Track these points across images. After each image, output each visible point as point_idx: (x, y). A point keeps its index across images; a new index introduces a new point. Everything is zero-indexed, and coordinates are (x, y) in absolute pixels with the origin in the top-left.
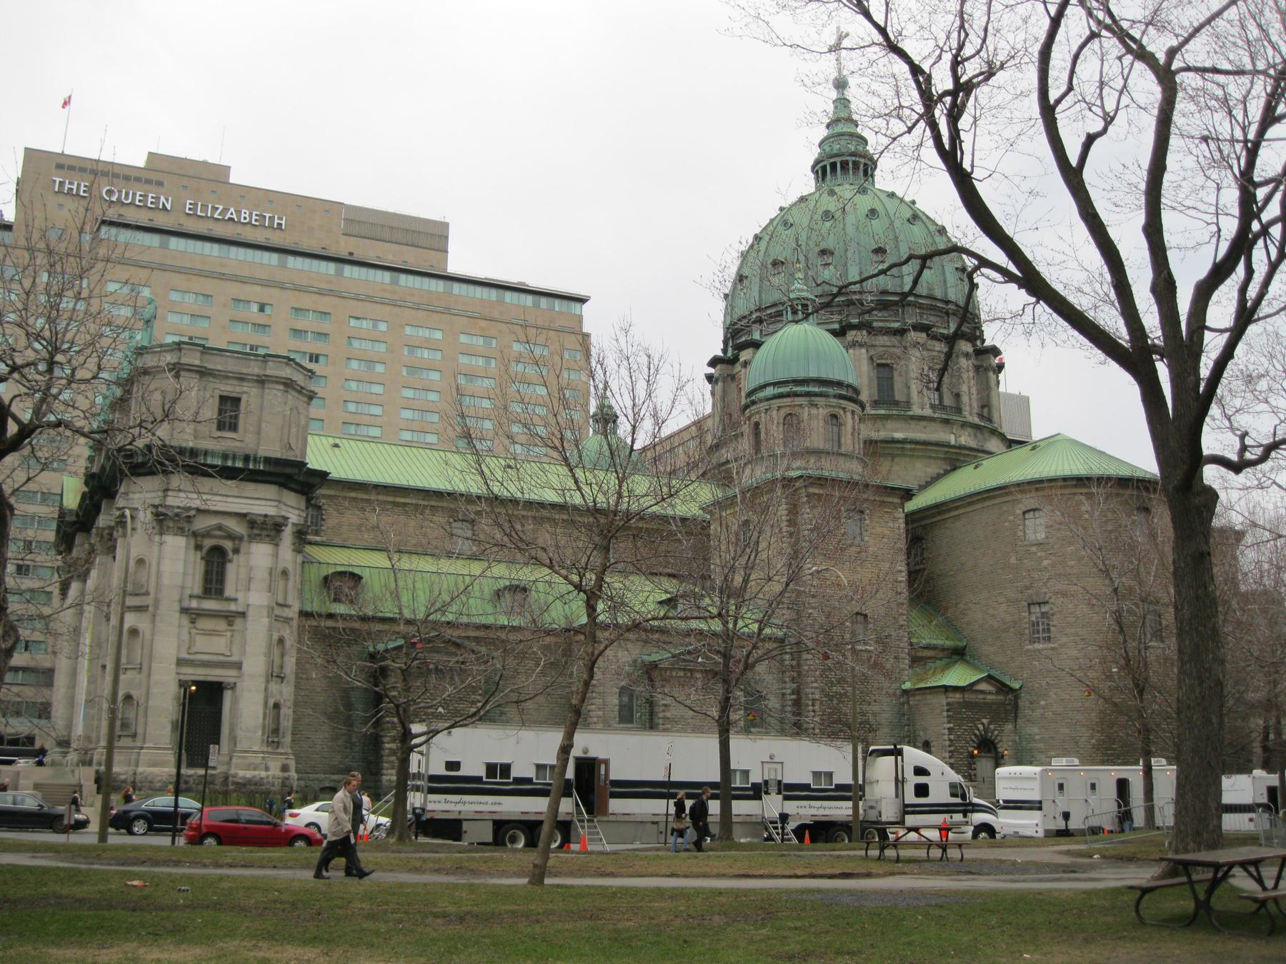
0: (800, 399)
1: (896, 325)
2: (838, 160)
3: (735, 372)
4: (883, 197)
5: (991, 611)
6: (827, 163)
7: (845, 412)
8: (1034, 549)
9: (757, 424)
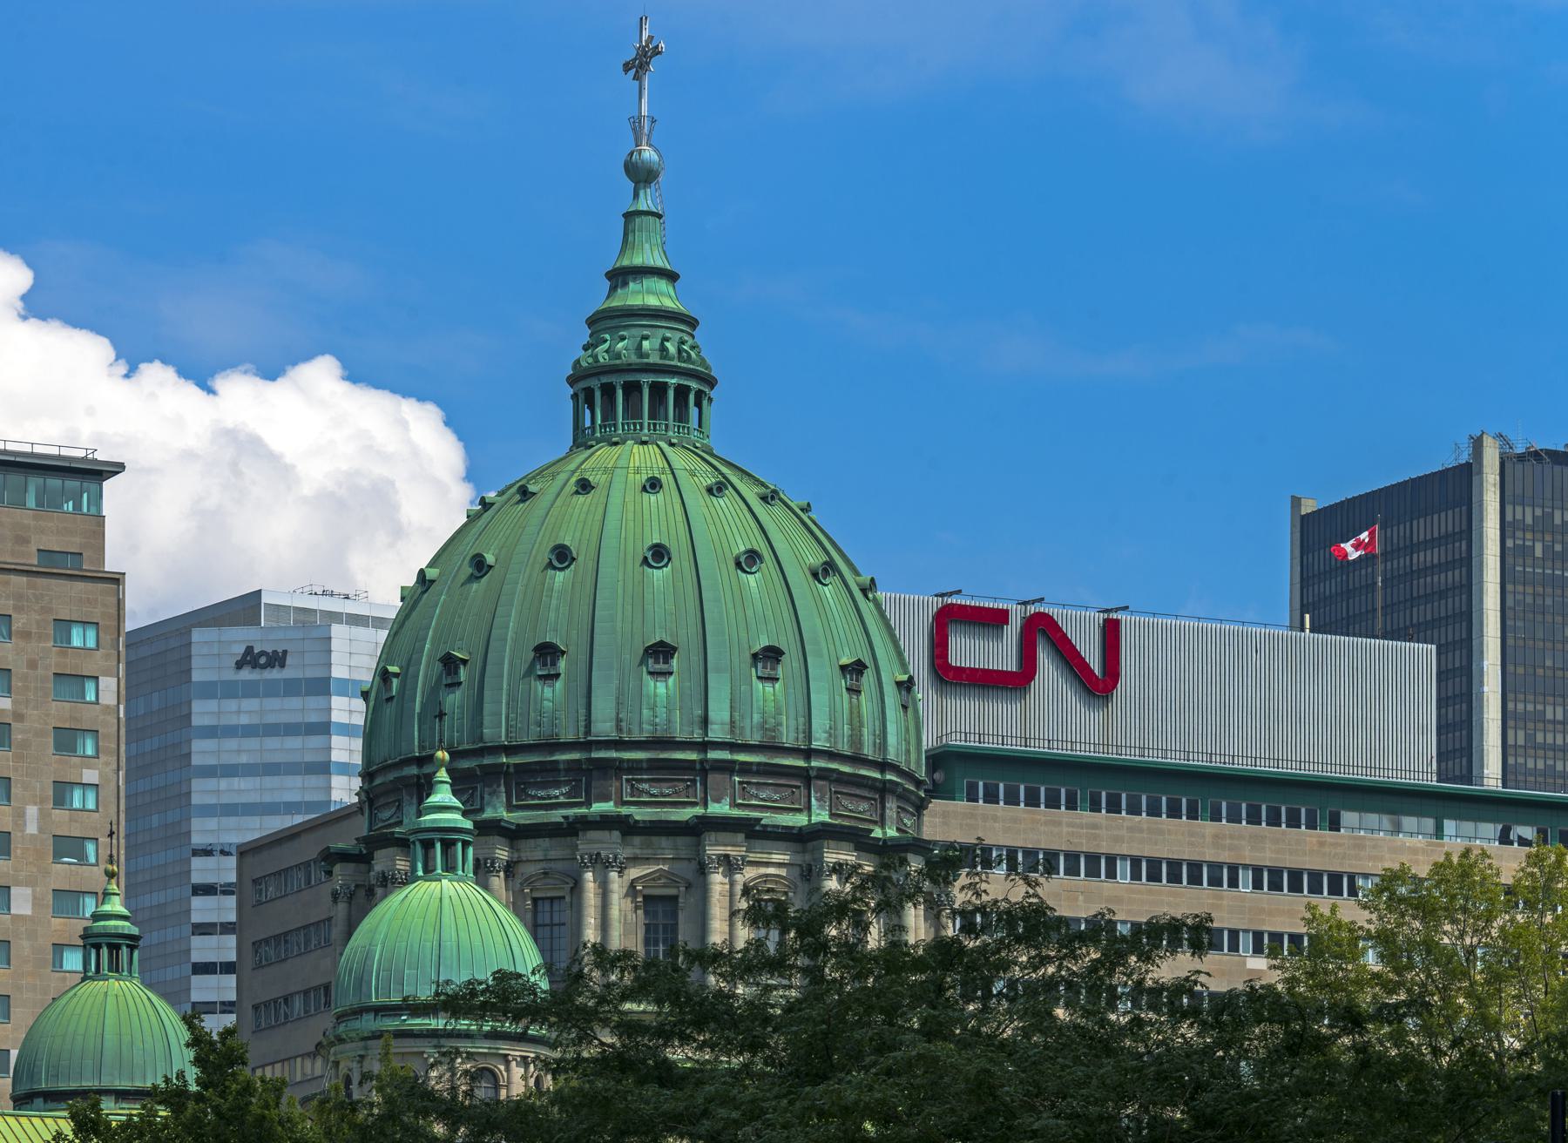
0: (419, 1042)
1: (686, 814)
2: (618, 380)
7: (507, 1063)
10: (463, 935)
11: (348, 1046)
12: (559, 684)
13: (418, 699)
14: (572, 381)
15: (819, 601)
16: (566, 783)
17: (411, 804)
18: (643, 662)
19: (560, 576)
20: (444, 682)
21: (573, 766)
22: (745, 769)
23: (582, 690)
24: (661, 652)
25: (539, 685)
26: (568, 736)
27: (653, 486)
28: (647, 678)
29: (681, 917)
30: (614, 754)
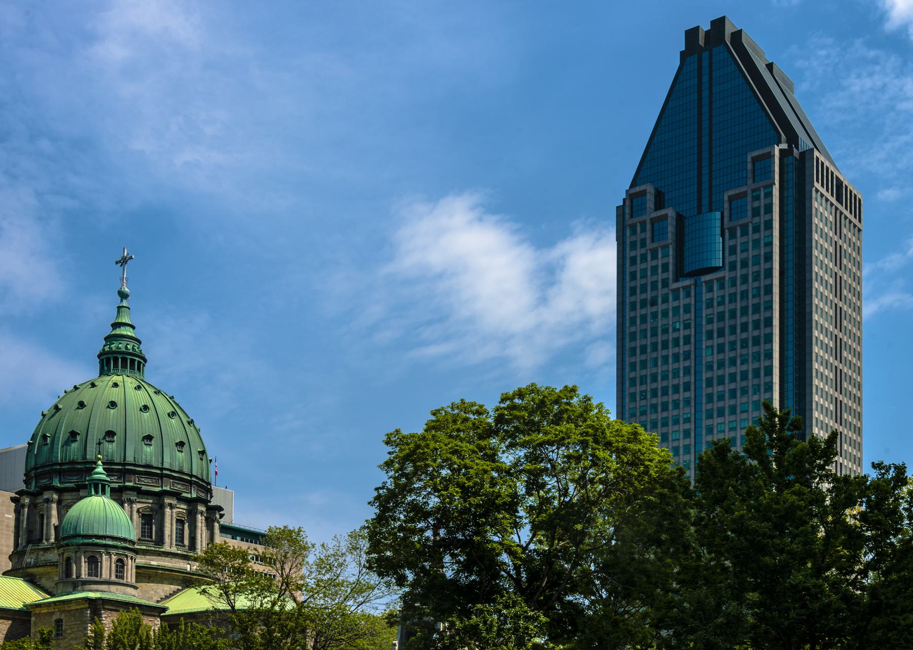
7: (127, 558)
10: (113, 514)
11: (71, 548)
12: (114, 444)
13: (60, 444)
14: (99, 356)
15: (191, 430)
16: (116, 475)
17: (56, 478)
18: (143, 440)
19: (112, 411)
20: (71, 439)
21: (118, 471)
22: (174, 478)
23: (123, 447)
24: (149, 438)
25: (107, 443)
26: (117, 460)
27: (139, 388)
28: (144, 445)
30: (132, 468)
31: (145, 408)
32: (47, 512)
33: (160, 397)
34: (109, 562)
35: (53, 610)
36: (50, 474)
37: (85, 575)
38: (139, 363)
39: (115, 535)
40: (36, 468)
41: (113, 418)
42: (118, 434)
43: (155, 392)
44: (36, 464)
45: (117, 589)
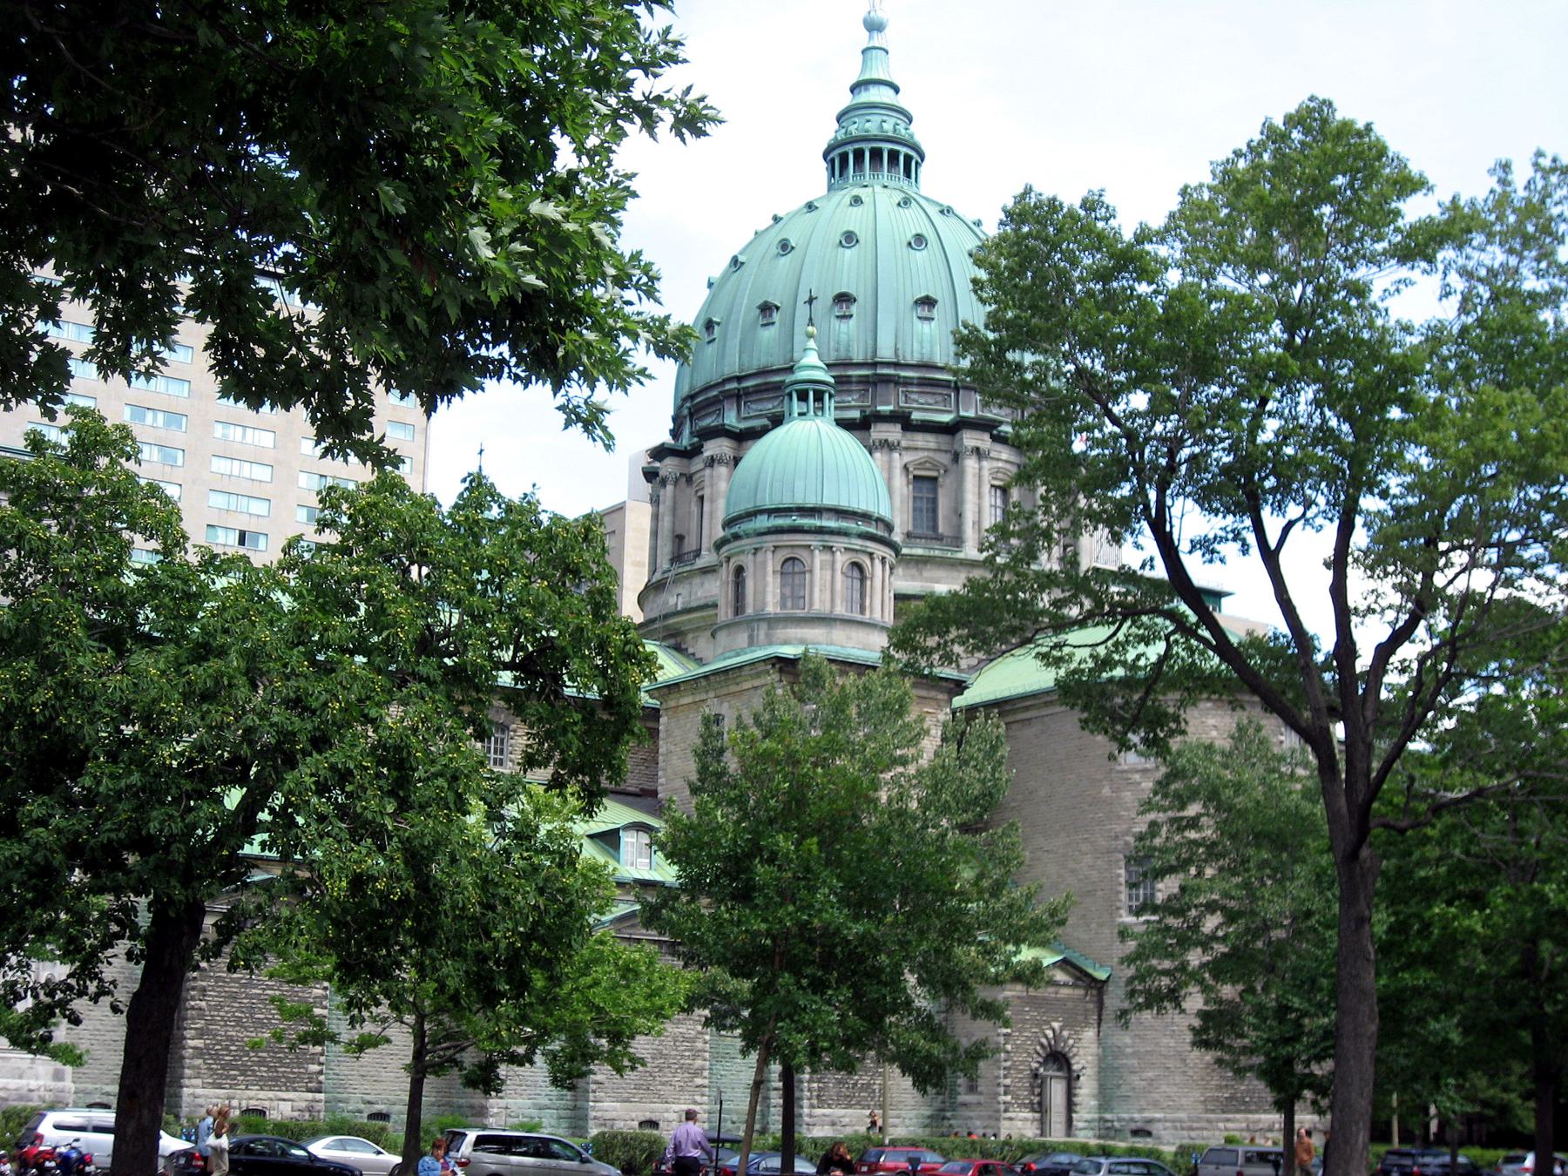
0: (807, 537)
1: (946, 418)
2: (867, 147)
3: (693, 470)
4: (933, 212)
5: (1071, 865)
6: (850, 149)
7: (872, 559)
8: (1137, 777)
9: (739, 570)
12: (852, 322)
19: (848, 252)
21: (864, 381)
24: (928, 302)
25: (837, 322)
26: (858, 357)
29: (941, 492)
31: (920, 239)
32: (712, 486)
33: (952, 220)
34: (829, 573)
35: (703, 696)
36: (715, 404)
37: (775, 605)
38: (908, 159)
39: (844, 503)
40: (692, 397)
41: (848, 271)
42: (860, 299)
43: (942, 212)
44: (691, 387)
45: (849, 638)
